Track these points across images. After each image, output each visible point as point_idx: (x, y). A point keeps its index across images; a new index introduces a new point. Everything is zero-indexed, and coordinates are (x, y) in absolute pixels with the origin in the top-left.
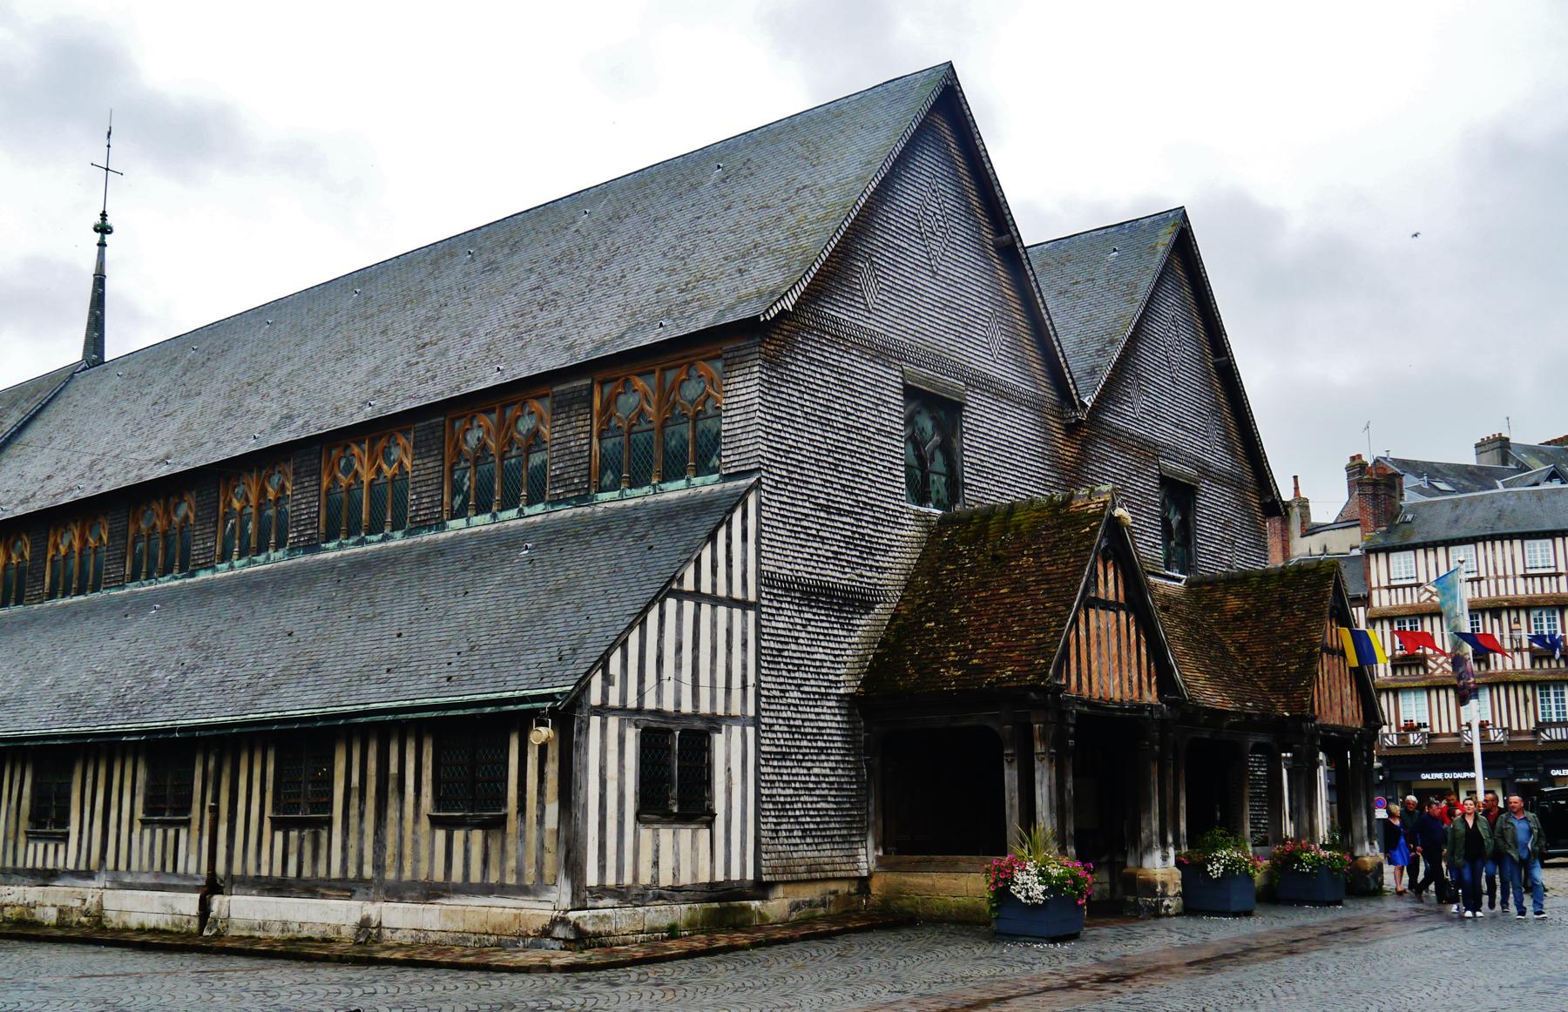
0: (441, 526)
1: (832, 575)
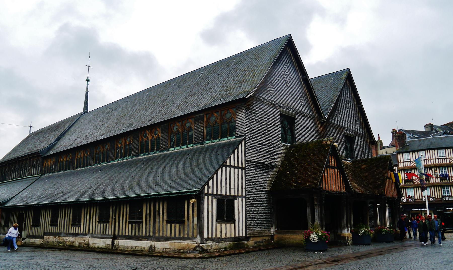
0: (168, 150)
1: (264, 161)
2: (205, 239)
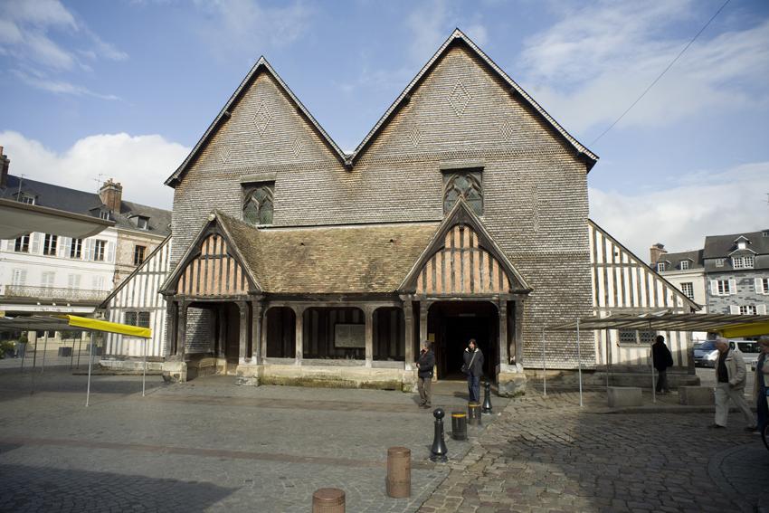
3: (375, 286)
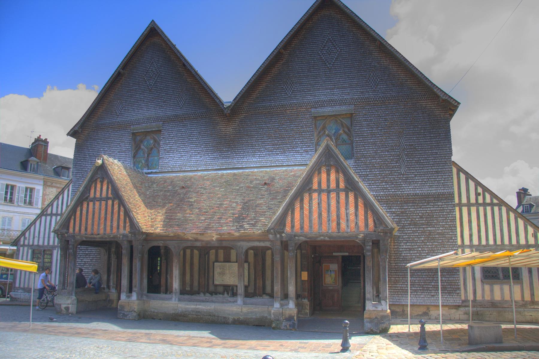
2: (17, 288)
3: (246, 226)
